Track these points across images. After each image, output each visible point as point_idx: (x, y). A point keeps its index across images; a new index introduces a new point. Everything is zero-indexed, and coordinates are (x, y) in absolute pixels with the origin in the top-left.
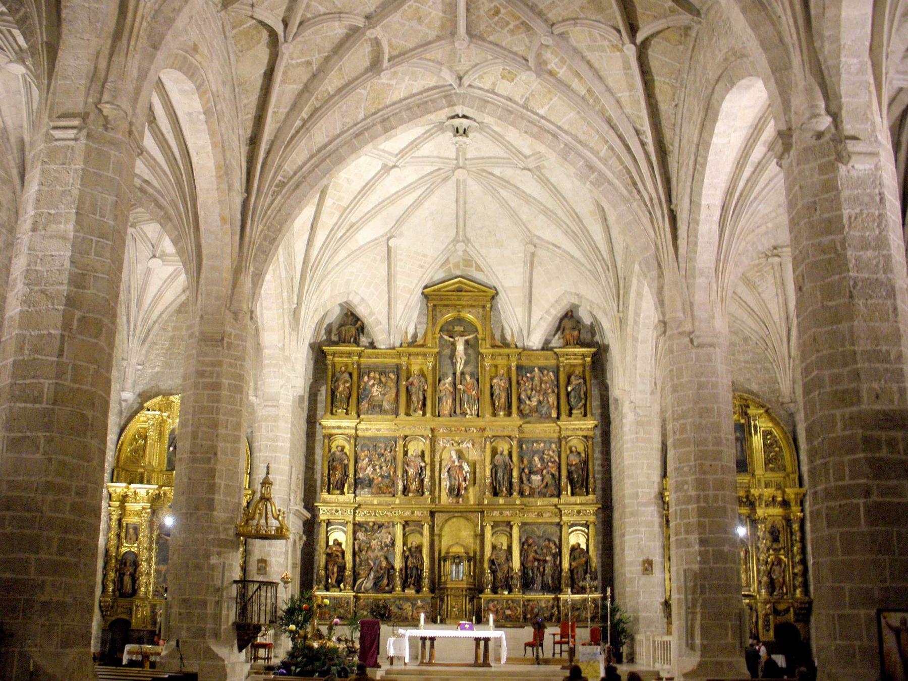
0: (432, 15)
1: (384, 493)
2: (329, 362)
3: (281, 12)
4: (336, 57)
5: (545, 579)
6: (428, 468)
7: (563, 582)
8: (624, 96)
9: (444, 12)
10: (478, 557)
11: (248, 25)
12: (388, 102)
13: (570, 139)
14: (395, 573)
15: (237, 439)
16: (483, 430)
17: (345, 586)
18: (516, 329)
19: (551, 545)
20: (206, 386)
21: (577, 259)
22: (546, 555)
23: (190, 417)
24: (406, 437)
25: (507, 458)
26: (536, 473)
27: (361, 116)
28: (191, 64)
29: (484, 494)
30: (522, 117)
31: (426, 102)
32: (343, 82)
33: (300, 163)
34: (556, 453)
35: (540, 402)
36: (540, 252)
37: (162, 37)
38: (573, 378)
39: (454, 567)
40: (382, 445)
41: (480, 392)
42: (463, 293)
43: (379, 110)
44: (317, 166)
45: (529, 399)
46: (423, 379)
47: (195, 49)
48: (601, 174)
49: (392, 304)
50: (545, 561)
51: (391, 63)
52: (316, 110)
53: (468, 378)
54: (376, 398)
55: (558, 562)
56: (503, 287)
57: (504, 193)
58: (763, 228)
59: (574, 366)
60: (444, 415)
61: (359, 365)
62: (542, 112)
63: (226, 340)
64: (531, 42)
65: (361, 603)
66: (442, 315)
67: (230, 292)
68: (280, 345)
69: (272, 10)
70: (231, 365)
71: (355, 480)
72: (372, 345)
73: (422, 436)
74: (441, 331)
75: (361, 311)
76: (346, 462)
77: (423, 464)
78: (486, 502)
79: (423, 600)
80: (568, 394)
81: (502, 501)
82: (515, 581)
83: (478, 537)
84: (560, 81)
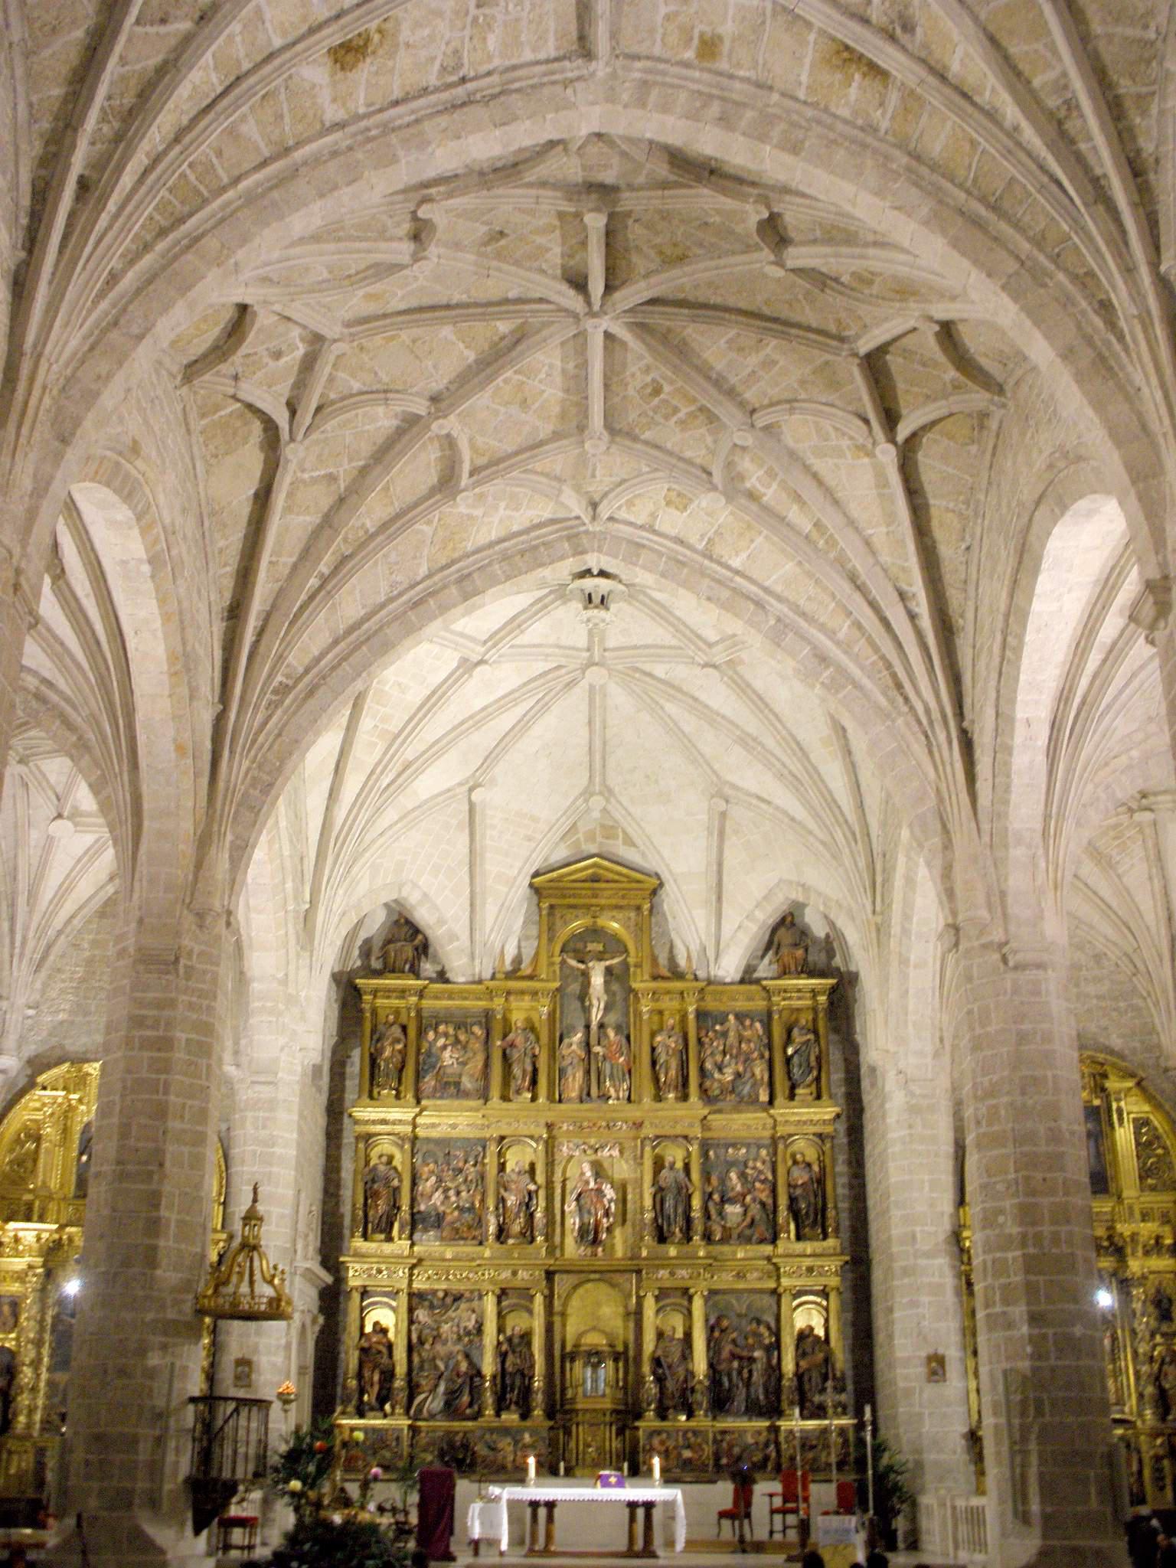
0: (545, 395)
1: (465, 1239)
2: (366, 1006)
3: (284, 389)
4: (379, 469)
5: (752, 1390)
6: (542, 1193)
7: (784, 1397)
8: (878, 533)
9: (567, 391)
10: (631, 1353)
11: (229, 410)
12: (470, 547)
13: (786, 610)
14: (483, 1384)
15: (200, 1139)
16: (639, 1125)
17: (393, 1407)
18: (694, 948)
19: (763, 1329)
20: (146, 1044)
21: (800, 823)
22: (752, 1348)
23: (117, 1098)
24: (502, 1138)
25: (682, 1175)
26: (732, 1201)
27: (423, 571)
28: (127, 475)
29: (642, 1238)
30: (702, 573)
31: (536, 547)
32: (391, 511)
33: (316, 653)
34: (769, 1164)
35: (738, 1075)
36: (737, 812)
37: (77, 422)
38: (796, 1032)
39: (589, 1371)
40: (461, 1154)
41: (633, 1059)
42: (603, 885)
43: (453, 562)
44: (344, 659)
45: (720, 1069)
46: (532, 1037)
47: (135, 449)
48: (841, 670)
49: (478, 902)
50: (752, 1360)
51: (475, 478)
52: (344, 559)
53: (611, 1033)
54: (449, 1071)
55: (774, 1361)
56: (670, 872)
57: (671, 708)
58: (1124, 760)
59: (799, 1010)
60: (570, 1100)
61: (419, 1011)
62: (736, 563)
63: (182, 961)
64: (715, 442)
65: (423, 1439)
66: (566, 923)
67: (191, 877)
68: (281, 975)
69: (270, 387)
70: (191, 1006)
71: (413, 1215)
72: (442, 977)
73: (531, 1137)
75: (423, 916)
76: (396, 1183)
77: (532, 1187)
78: (644, 1253)
79: (533, 1432)
80: (788, 1060)
81: (673, 1251)
82: (698, 1397)
83: (632, 1317)
84: (766, 509)
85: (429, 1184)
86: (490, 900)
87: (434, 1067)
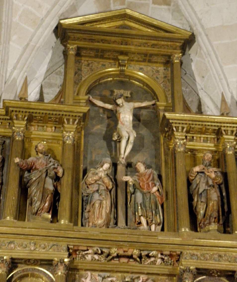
56: (202, 26)
74: (89, 92)
86: (14, 38)
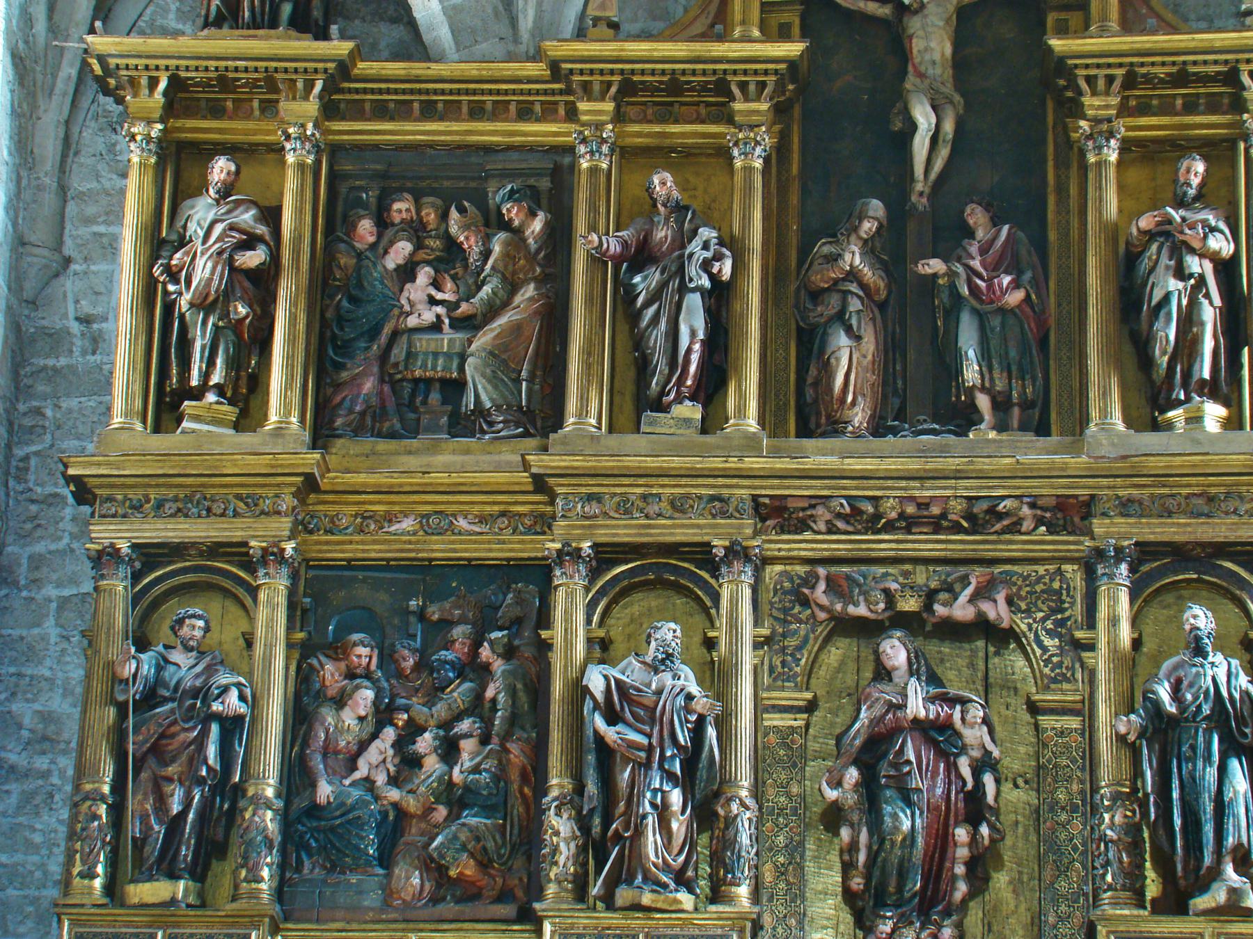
54: (423, 343)
85: (349, 718)
87: (374, 333)
